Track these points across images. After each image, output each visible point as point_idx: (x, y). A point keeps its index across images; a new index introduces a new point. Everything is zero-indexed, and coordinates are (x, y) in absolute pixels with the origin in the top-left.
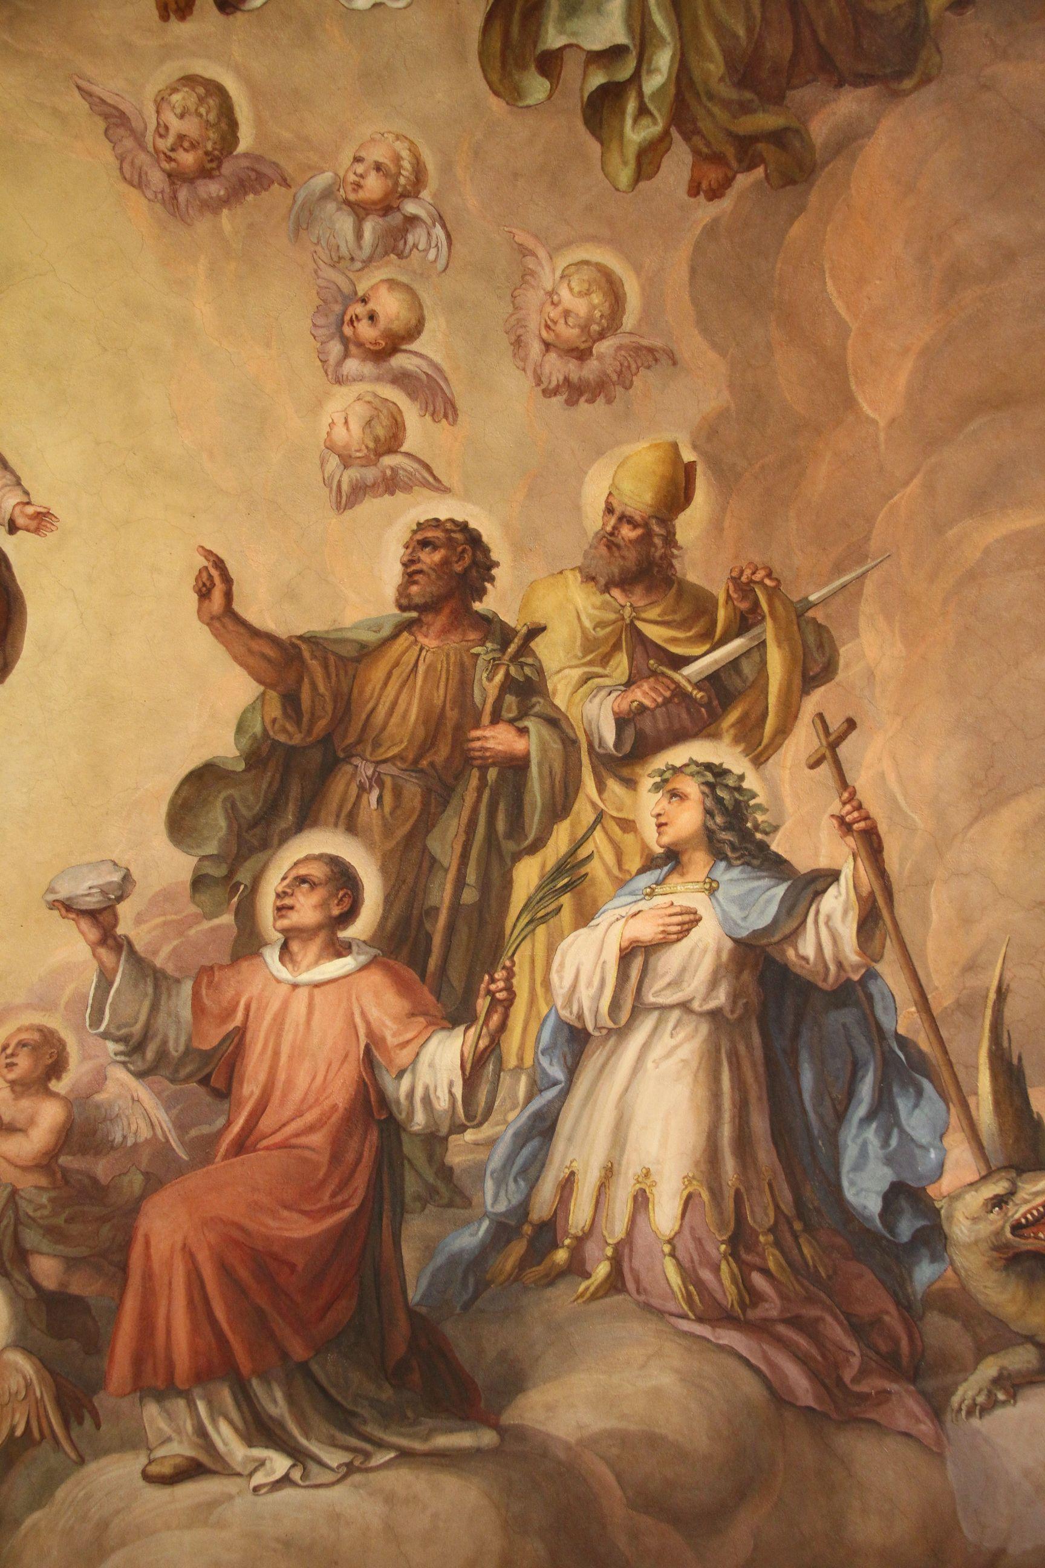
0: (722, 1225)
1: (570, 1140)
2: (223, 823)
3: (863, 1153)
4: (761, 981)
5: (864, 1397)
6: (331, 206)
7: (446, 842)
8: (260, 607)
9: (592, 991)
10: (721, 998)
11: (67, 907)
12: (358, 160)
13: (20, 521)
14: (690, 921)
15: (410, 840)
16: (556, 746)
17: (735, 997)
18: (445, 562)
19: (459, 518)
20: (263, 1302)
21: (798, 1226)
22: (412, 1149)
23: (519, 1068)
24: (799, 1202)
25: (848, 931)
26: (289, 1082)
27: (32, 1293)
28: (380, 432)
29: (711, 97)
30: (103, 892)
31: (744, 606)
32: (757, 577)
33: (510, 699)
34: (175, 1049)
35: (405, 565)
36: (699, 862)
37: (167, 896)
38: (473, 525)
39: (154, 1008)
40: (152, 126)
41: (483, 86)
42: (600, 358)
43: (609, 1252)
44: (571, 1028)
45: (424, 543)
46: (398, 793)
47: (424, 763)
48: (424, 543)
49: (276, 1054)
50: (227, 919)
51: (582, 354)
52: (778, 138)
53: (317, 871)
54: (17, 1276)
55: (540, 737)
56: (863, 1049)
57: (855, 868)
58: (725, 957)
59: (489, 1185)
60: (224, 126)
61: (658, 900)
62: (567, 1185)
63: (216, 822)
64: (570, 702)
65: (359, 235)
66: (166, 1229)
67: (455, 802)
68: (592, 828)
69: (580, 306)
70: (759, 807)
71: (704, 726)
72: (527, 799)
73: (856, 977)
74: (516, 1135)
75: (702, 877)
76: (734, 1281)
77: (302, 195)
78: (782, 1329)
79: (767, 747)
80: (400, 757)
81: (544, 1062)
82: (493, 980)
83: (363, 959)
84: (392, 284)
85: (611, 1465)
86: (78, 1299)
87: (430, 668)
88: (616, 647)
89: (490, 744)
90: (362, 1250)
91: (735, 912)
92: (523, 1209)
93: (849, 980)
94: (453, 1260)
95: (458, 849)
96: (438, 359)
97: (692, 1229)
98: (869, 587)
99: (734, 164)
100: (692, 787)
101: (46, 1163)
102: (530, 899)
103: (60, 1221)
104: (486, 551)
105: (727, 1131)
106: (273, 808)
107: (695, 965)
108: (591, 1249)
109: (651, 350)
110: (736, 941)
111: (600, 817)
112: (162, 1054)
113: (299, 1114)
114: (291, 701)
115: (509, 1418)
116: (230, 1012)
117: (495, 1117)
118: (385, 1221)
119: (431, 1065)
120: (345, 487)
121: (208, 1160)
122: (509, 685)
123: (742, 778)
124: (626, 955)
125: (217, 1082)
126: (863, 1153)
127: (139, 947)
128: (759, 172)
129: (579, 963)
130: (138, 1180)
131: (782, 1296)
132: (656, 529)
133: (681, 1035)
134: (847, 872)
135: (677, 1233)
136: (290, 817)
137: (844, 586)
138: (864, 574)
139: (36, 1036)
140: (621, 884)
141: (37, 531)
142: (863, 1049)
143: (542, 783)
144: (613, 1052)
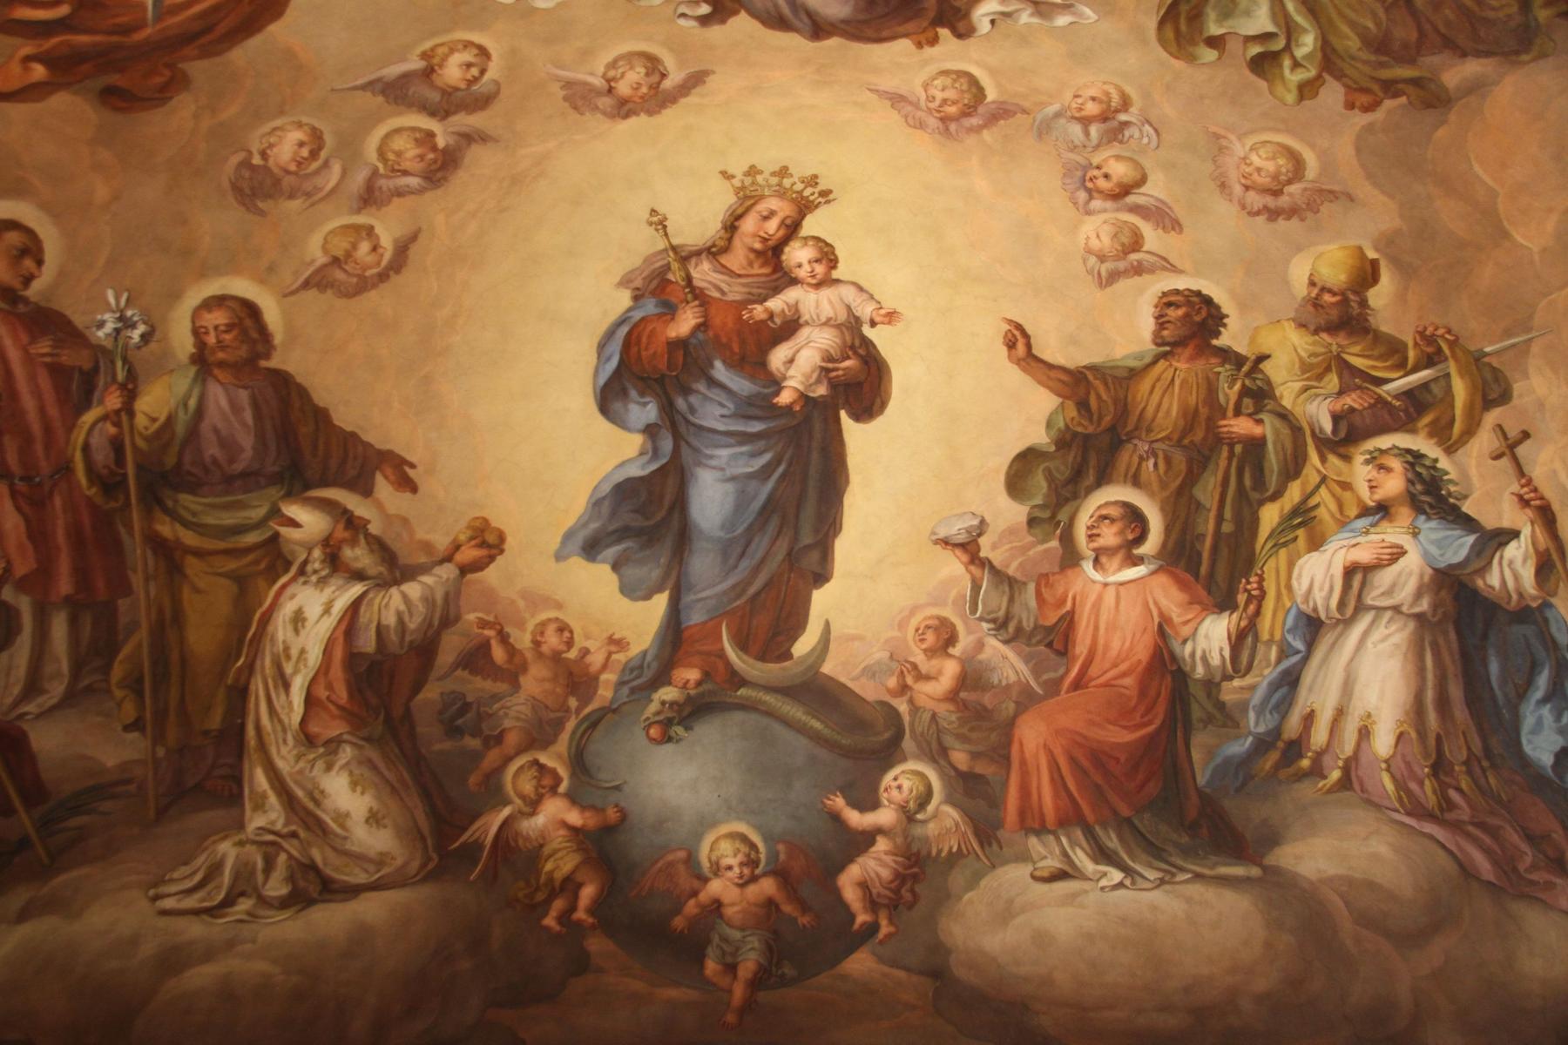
0: (1426, 755)
1: (1310, 690)
2: (1044, 484)
3: (1539, 722)
4: (1456, 598)
5: (1532, 883)
6: (1062, 121)
7: (1207, 491)
8: (1051, 349)
9: (1324, 594)
10: (1424, 605)
11: (946, 542)
12: (1076, 96)
13: (877, 319)
14: (1398, 553)
15: (1180, 491)
16: (1286, 431)
17: (1435, 606)
18: (1187, 315)
19: (1194, 288)
20: (1099, 779)
21: (1485, 764)
22: (1197, 692)
23: (1271, 641)
24: (1487, 751)
25: (1528, 574)
26: (1107, 647)
27: (953, 773)
28: (1125, 240)
29: (1353, 58)
30: (968, 532)
31: (1430, 350)
32: (1440, 332)
33: (1247, 401)
34: (1028, 625)
35: (1157, 318)
36: (1404, 514)
37: (1011, 531)
38: (1205, 292)
39: (1011, 600)
40: (923, 96)
41: (1164, 55)
42: (1290, 195)
43: (1341, 763)
44: (1309, 617)
45: (1169, 304)
46: (1168, 461)
47: (1186, 441)
48: (1169, 304)
49: (1096, 628)
50: (1054, 543)
51: (1276, 193)
52: (1416, 82)
53: (1114, 512)
54: (942, 762)
55: (1273, 426)
56: (1540, 653)
57: (1533, 531)
58: (1426, 579)
59: (1252, 715)
60: (974, 90)
61: (1372, 537)
62: (1309, 718)
63: (1039, 484)
64: (1294, 403)
65: (1087, 134)
66: (1032, 735)
67: (1211, 467)
68: (1318, 486)
69: (1270, 166)
70: (1451, 481)
71: (1405, 424)
72: (1266, 465)
73: (1534, 605)
74: (1270, 684)
75: (1407, 523)
76: (1434, 792)
77: (1039, 117)
78: (1470, 828)
79: (1456, 442)
80: (1168, 438)
81: (1290, 638)
82: (1248, 583)
83: (1152, 567)
84: (1118, 158)
85: (1342, 897)
86: (980, 777)
87: (1184, 382)
88: (1328, 369)
89: (1235, 429)
90: (1162, 757)
91: (1434, 550)
92: (1277, 732)
93: (1528, 607)
94: (1227, 761)
95: (1217, 497)
96: (1162, 196)
97: (1403, 756)
98: (1535, 348)
99: (1381, 94)
100: (1396, 464)
101: (952, 697)
102: (1273, 531)
103: (964, 730)
104: (1218, 308)
105: (1430, 695)
106: (1078, 474)
107: (1406, 577)
108: (1327, 760)
109: (1331, 192)
110: (1436, 570)
111: (1324, 479)
112: (1019, 630)
113: (1115, 665)
114: (1083, 405)
115: (1270, 860)
116: (1063, 602)
117: (1255, 671)
118: (1179, 734)
119: (1206, 636)
120: (1104, 274)
121: (1057, 693)
122: (1245, 391)
123: (1436, 460)
124: (1349, 572)
125: (1058, 645)
126: (1539, 722)
127: (996, 563)
128: (1403, 99)
129: (1315, 574)
130: (1012, 706)
131: (1471, 807)
132: (1352, 297)
133: (1393, 628)
134: (1526, 532)
135: (1392, 756)
136: (1091, 478)
137: (1513, 345)
138: (1530, 340)
139: (936, 622)
140: (1343, 524)
141: (889, 323)
142: (1540, 653)
143: (1276, 453)
144: (1341, 635)
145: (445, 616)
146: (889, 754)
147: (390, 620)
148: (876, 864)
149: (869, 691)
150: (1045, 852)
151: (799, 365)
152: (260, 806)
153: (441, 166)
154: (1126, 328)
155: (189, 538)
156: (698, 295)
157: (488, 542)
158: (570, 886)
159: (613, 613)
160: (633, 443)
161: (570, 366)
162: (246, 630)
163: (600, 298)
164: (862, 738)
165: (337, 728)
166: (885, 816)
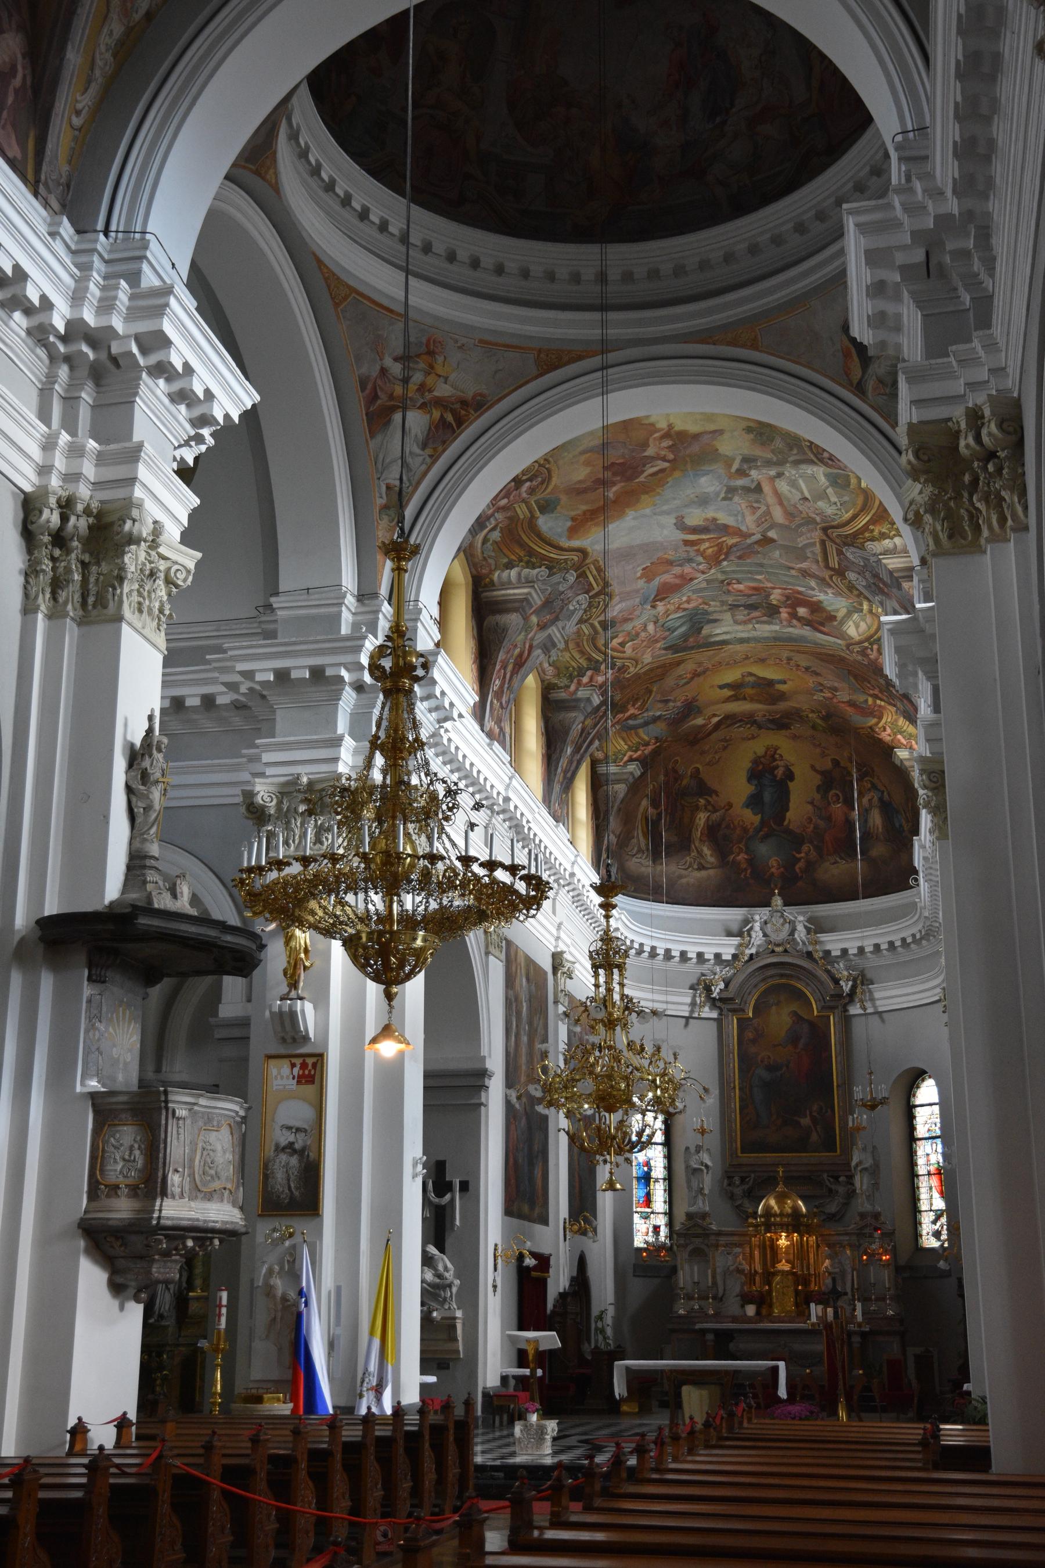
8: (818, 768)
145: (723, 819)
148: (801, 865)
151: (780, 772)
153: (725, 748)
154: (828, 765)
157: (730, 805)
159: (751, 818)
160: (753, 788)
161: (742, 777)
162: (692, 820)
163: (746, 764)
164: (796, 840)
166: (802, 855)
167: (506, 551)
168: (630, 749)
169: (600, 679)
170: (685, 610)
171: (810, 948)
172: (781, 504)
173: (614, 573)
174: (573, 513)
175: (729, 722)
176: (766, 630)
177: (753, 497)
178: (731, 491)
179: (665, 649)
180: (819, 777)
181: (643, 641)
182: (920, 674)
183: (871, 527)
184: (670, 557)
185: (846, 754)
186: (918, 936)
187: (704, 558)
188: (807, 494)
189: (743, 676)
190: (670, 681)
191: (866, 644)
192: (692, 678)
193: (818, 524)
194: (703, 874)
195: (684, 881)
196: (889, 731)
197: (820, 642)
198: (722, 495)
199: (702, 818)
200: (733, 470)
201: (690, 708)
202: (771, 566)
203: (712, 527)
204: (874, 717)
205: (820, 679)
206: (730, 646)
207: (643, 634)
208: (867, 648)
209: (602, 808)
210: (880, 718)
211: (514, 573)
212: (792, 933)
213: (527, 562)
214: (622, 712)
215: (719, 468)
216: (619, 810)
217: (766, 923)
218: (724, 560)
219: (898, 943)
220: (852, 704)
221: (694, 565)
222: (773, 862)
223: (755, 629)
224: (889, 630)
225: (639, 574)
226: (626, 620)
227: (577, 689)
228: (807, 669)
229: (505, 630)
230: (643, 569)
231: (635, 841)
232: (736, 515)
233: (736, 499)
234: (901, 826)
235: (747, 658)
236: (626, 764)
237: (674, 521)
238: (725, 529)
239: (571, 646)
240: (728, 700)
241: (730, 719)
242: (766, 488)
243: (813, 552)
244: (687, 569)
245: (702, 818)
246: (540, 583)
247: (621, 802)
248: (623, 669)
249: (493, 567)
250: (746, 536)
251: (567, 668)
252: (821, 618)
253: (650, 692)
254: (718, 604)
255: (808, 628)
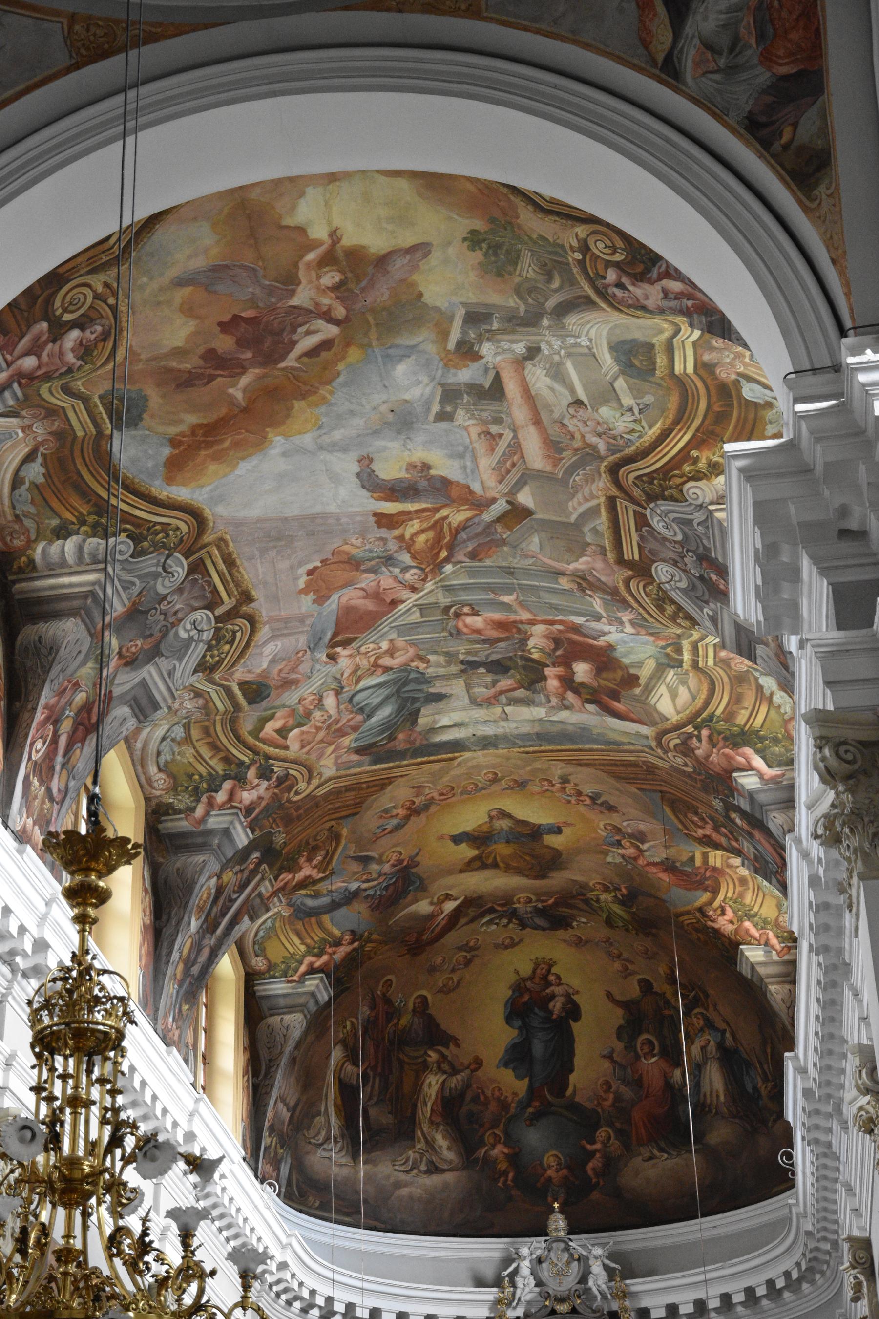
11: (604, 1057)
62: (705, 1095)
66: (636, 1115)
101: (613, 1105)
145: (467, 1085)
146: (596, 1126)
147: (453, 1086)
149: (589, 1105)
150: (645, 1152)
151: (556, 1006)
152: (419, 1141)
153: (468, 963)
154: (634, 991)
155: (406, 1059)
156: (528, 990)
157: (478, 1063)
158: (505, 1173)
159: (513, 1085)
160: (516, 1032)
163: (503, 992)
165: (438, 1119)
166: (598, 1146)
167: (55, 504)
168: (309, 951)
169: (247, 797)
170: (387, 669)
171: (615, 1306)
172: (537, 422)
173: (255, 572)
174: (173, 430)
175: (472, 912)
176: (525, 717)
177: (489, 409)
178: (451, 395)
179: (359, 751)
180: (620, 1012)
181: (318, 729)
182: (806, 563)
183: (694, 453)
184: (354, 551)
185: (662, 970)
186: (795, 1275)
187: (414, 557)
188: (582, 395)
189: (491, 818)
190: (369, 821)
191: (690, 729)
192: (407, 818)
193: (602, 459)
194: (436, 1180)
195: (404, 1192)
196: (730, 914)
197: (612, 736)
198: (436, 408)
199: (433, 1084)
200: (451, 345)
201: (407, 880)
202: (527, 573)
203: (423, 484)
204: (706, 890)
205: (615, 819)
206: (467, 755)
207: (317, 714)
208: (690, 736)
209: (264, 1054)
210: (715, 891)
211: (70, 545)
212: (583, 1280)
213: (95, 525)
214: (289, 871)
215: (423, 338)
216: (293, 1060)
217: (540, 1261)
218: (447, 560)
219: (761, 1291)
220: (669, 866)
221: (397, 571)
222: (550, 1159)
223: (505, 717)
224: (741, 470)
225: (301, 584)
226: (287, 684)
227: (207, 814)
228: (594, 798)
229: (53, 649)
230: (310, 573)
231: (321, 1119)
232: (461, 456)
233: (461, 416)
234: (755, 1088)
235: (495, 780)
236: (302, 980)
237: (356, 468)
238: (445, 489)
239: (195, 733)
240: (469, 866)
241: (474, 907)
242: (511, 387)
243: (595, 531)
244: (385, 580)
245: (433, 1084)
246: (118, 566)
247: (297, 1046)
248: (285, 782)
249: (33, 537)
250: (481, 504)
251: (190, 776)
252: (613, 686)
253: (337, 837)
254: (442, 659)
255: (591, 707)
